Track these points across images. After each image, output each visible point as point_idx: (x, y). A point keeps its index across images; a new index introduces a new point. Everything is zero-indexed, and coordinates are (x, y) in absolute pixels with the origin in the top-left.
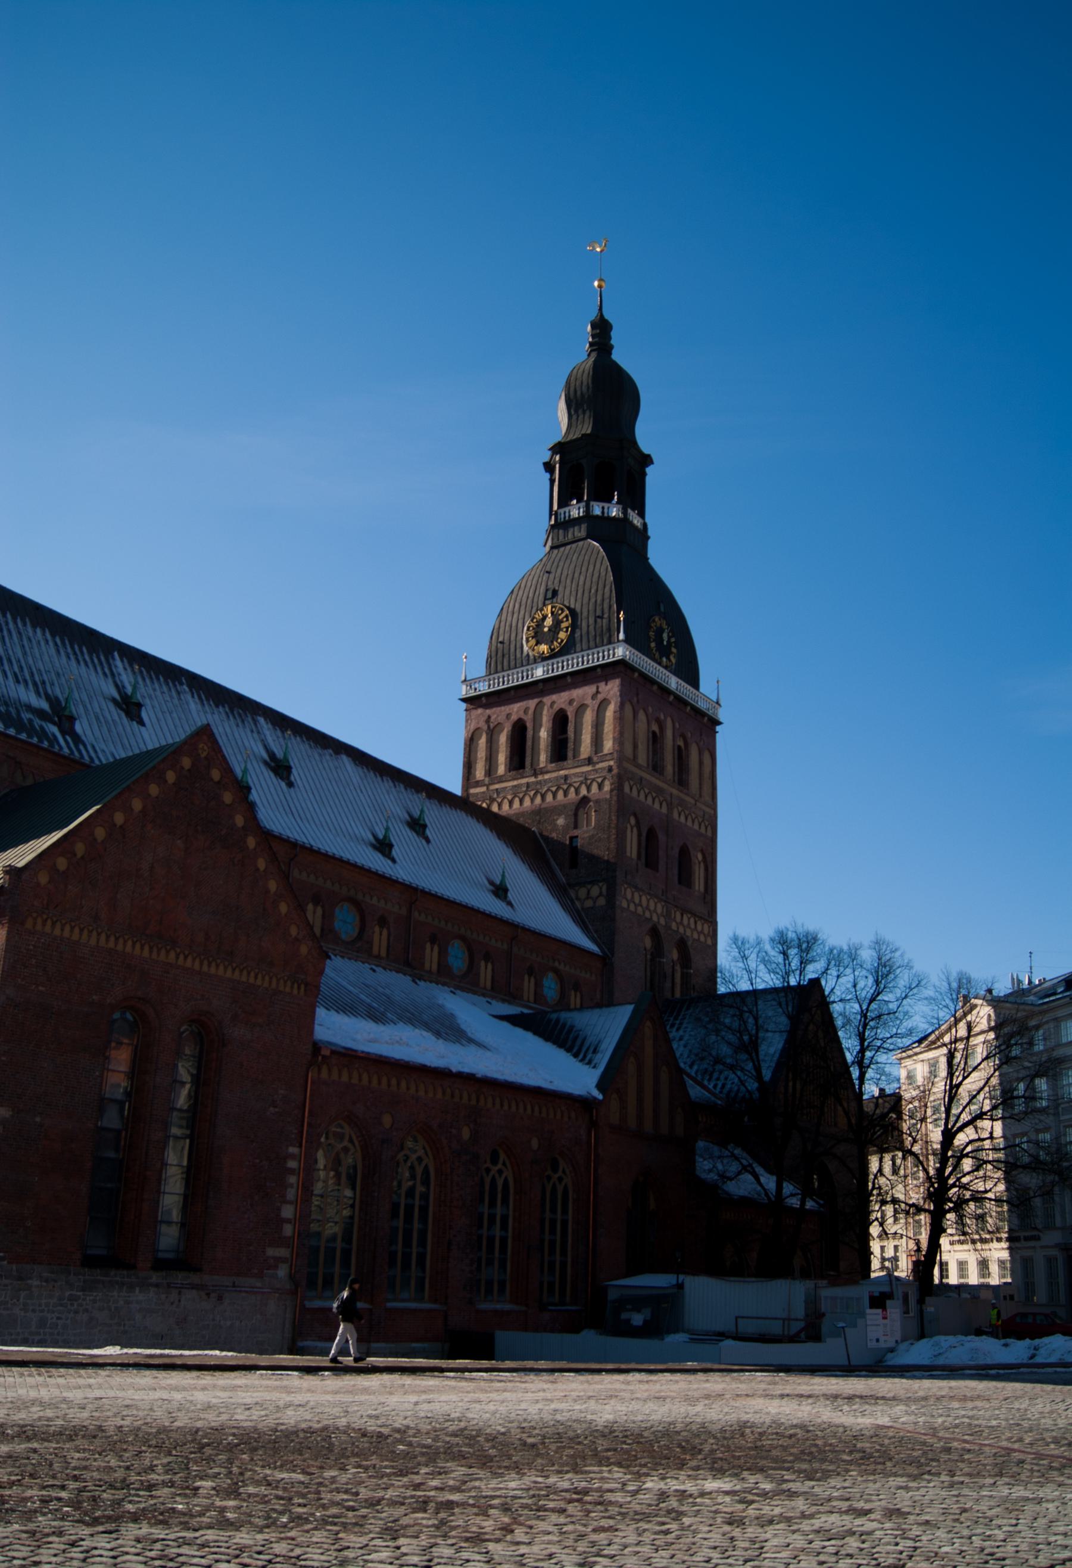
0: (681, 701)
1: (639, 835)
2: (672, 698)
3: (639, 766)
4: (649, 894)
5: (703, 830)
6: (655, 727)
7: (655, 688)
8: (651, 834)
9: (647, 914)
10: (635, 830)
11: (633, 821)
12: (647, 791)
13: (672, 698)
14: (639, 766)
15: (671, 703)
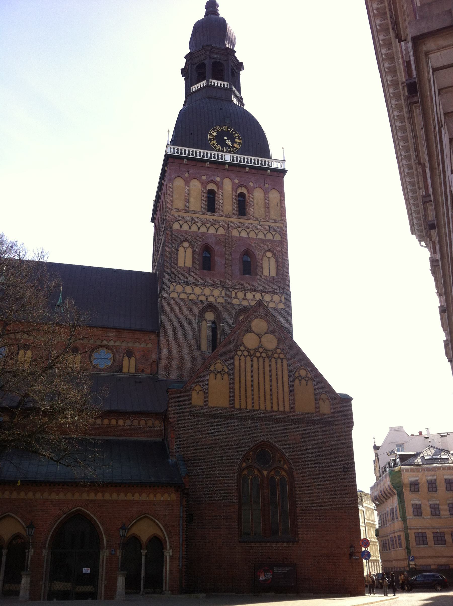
0: (235, 167)
1: (193, 252)
2: (227, 166)
3: (192, 212)
4: (203, 285)
5: (269, 237)
6: (210, 186)
7: (207, 164)
8: (207, 248)
9: (202, 298)
10: (189, 251)
11: (186, 244)
12: (199, 225)
13: (227, 166)
14: (192, 212)
15: (227, 170)
